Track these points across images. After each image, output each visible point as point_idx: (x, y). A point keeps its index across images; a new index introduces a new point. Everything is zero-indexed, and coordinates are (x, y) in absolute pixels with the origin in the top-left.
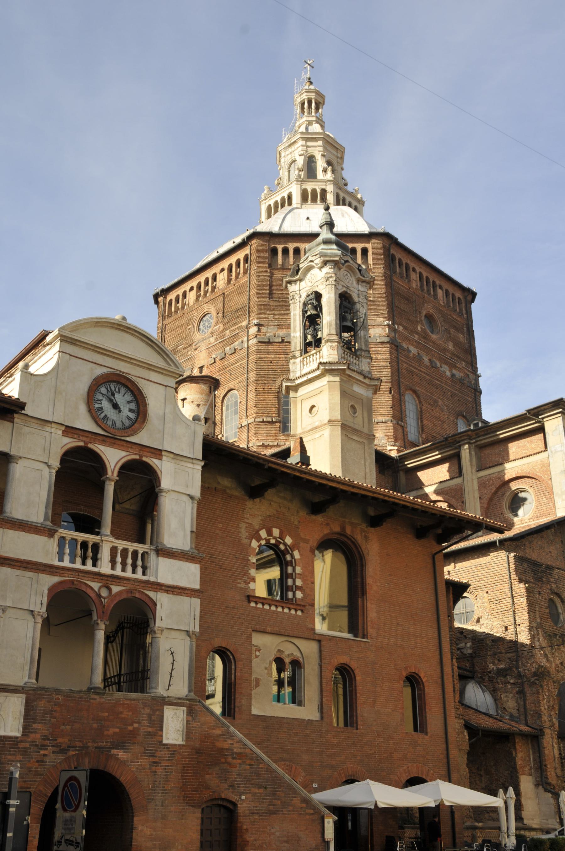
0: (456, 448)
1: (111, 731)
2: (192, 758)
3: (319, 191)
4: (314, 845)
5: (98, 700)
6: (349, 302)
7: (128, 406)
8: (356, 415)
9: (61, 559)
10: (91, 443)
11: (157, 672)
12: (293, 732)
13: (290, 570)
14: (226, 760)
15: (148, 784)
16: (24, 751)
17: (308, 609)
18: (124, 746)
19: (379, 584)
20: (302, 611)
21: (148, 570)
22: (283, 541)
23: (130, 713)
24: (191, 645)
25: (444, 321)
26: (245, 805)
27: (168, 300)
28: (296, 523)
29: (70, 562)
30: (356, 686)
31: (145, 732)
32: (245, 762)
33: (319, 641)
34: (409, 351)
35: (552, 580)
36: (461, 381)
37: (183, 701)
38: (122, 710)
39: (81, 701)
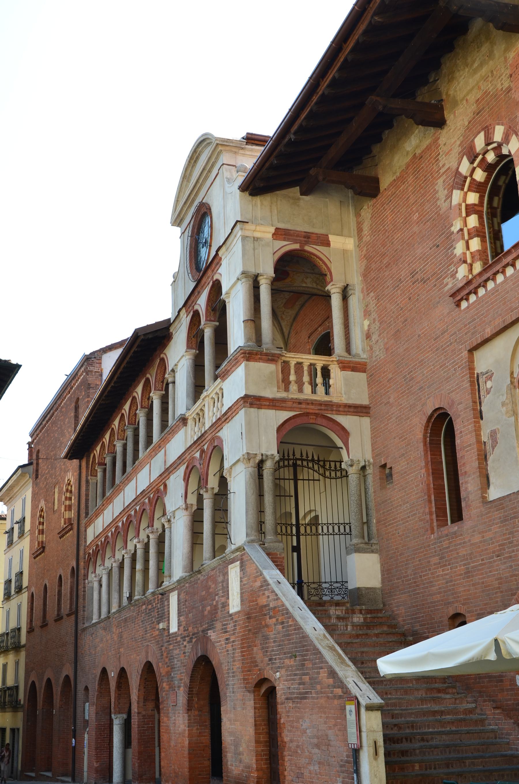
28: (506, 85)
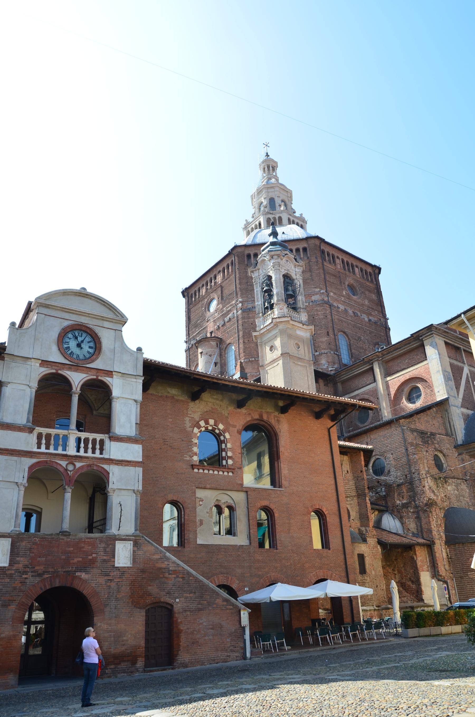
0: (370, 364)
1: (76, 560)
2: (138, 575)
3: (277, 218)
4: (233, 629)
5: (65, 539)
6: (290, 279)
7: (89, 345)
8: (300, 349)
9: (39, 447)
10: (60, 370)
11: (111, 519)
12: (228, 554)
13: (223, 446)
14: (164, 576)
15: (105, 594)
16: (11, 576)
17: (237, 471)
18: (85, 569)
19: (289, 451)
20: (233, 473)
21: (104, 451)
22: (217, 427)
23: (90, 547)
24: (136, 499)
25: (360, 287)
26: (179, 605)
27: (190, 294)
28: (226, 415)
29: (54, 450)
30: (275, 520)
31: (101, 559)
32: (178, 576)
33: (247, 492)
34: (338, 308)
35: (435, 442)
36: (375, 323)
37: (130, 537)
38: (83, 546)
39: (53, 541)
